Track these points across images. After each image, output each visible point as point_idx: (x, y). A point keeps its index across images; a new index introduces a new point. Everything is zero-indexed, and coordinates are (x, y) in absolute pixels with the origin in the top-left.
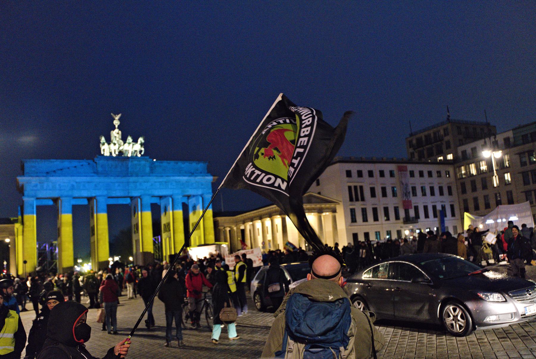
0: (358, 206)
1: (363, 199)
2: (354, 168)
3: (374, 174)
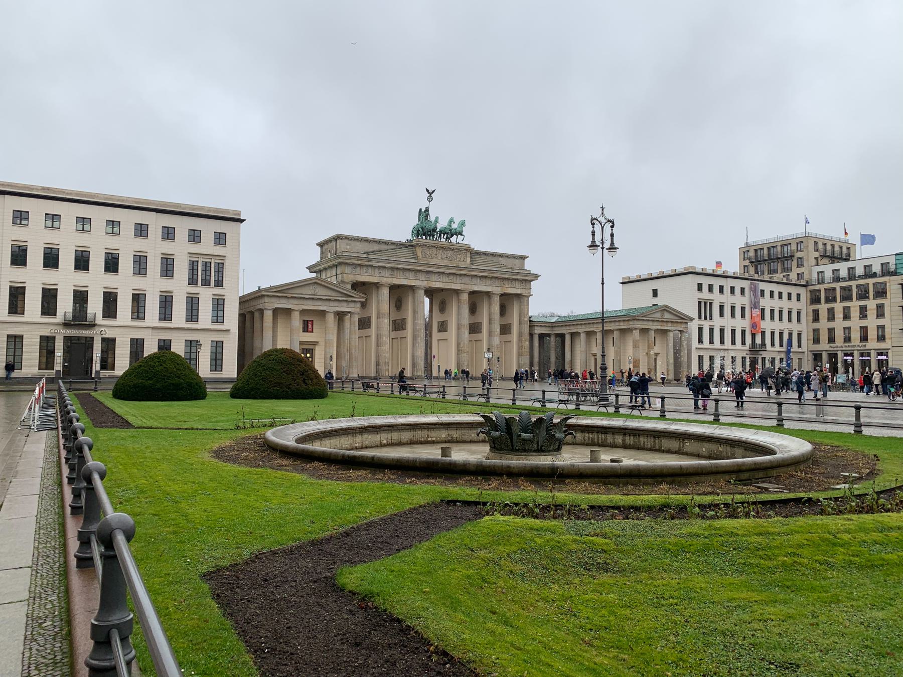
0: (706, 325)
1: (711, 319)
2: (706, 281)
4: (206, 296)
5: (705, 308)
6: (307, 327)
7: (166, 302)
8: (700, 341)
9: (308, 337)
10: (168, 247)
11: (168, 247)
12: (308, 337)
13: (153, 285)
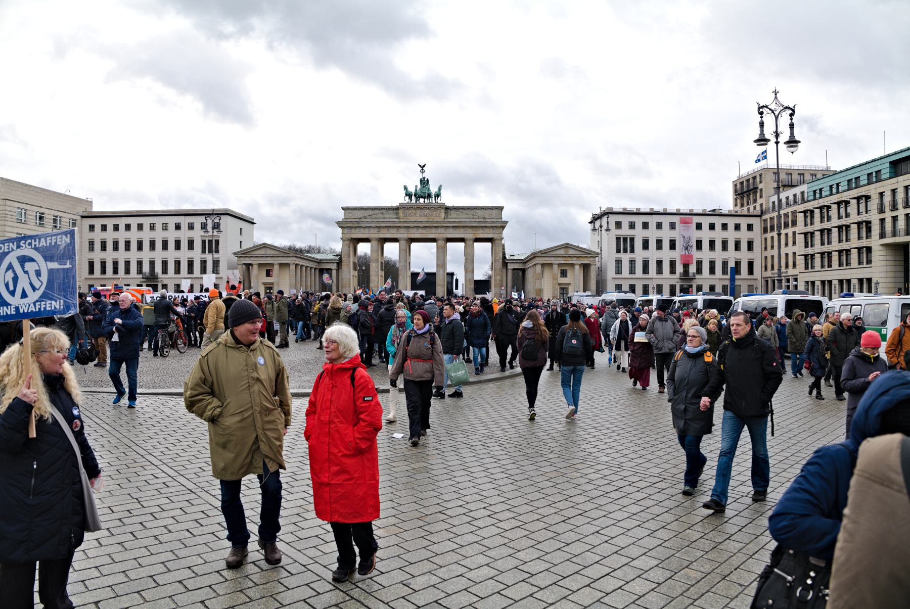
0: (625, 258)
1: (632, 251)
2: (625, 220)
3: (668, 225)
4: (209, 258)
5: (625, 244)
6: (268, 274)
7: (191, 264)
8: (619, 271)
9: (269, 280)
10: (191, 234)
11: (191, 234)
12: (269, 280)
13: (184, 255)
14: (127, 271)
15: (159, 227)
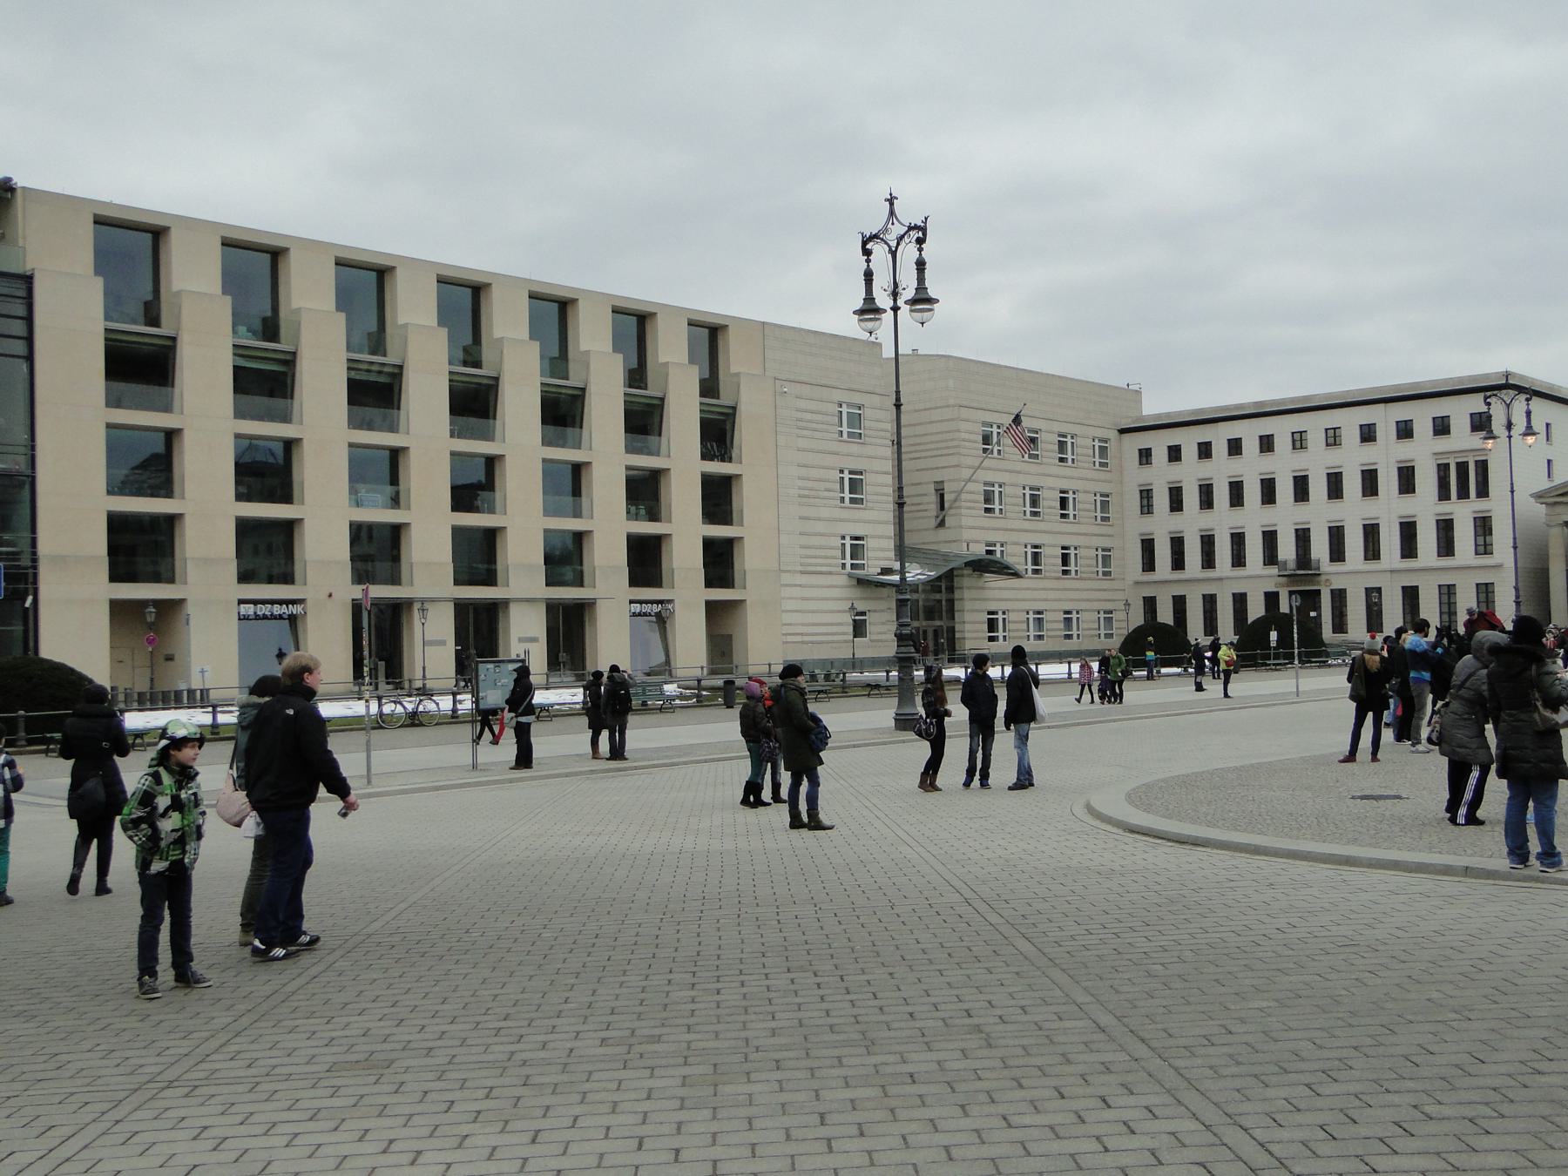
4: (1463, 513)
7: (1408, 531)
13: (1389, 508)
14: (1239, 560)
15: (1316, 439)
